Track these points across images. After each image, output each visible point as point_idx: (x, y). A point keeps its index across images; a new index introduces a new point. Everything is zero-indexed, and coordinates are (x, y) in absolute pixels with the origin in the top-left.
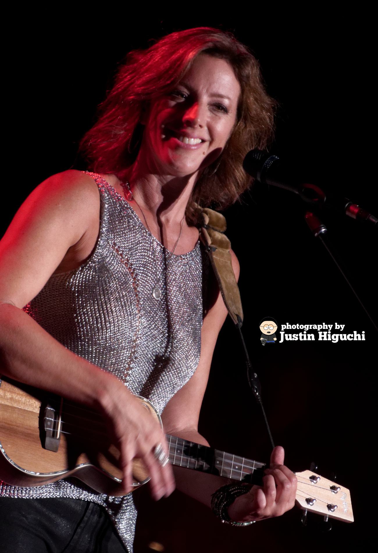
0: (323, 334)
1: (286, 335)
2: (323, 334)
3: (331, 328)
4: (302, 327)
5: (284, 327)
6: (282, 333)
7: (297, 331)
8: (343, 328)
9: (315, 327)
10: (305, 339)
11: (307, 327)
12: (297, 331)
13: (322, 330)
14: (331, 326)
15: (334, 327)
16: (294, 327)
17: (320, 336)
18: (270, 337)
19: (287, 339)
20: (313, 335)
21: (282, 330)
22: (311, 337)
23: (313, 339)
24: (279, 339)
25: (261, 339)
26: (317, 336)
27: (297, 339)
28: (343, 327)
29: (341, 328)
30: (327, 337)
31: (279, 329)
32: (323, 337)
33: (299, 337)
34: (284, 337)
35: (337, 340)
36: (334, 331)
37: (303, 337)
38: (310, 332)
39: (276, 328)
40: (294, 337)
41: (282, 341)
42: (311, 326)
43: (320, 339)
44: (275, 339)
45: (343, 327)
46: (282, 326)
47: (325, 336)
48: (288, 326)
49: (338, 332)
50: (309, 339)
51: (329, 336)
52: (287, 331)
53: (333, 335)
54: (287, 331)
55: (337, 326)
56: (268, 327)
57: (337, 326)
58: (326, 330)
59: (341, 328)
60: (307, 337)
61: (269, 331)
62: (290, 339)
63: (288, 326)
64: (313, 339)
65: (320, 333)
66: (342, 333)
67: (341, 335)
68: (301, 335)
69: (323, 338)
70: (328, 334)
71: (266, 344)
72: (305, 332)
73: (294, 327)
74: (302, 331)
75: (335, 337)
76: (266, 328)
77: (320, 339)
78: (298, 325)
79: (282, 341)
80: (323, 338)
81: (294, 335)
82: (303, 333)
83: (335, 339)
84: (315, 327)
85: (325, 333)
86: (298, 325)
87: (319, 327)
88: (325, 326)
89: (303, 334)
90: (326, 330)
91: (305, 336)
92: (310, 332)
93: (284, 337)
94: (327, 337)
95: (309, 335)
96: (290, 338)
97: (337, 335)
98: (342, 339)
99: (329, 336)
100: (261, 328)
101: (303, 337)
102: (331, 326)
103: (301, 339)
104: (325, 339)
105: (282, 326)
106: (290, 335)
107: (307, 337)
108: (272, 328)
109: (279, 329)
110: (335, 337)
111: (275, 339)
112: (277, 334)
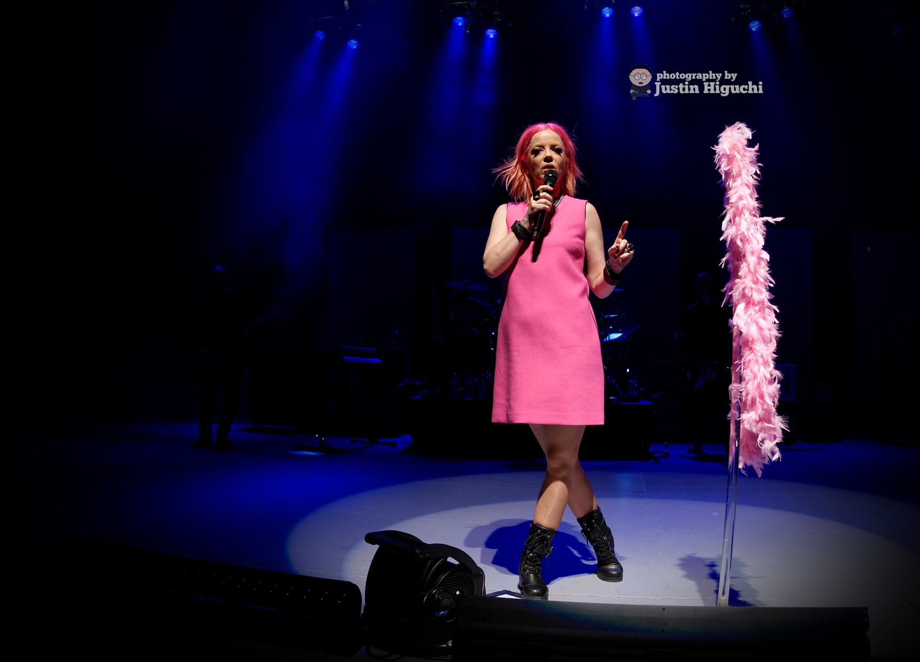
0: (709, 85)
1: (663, 87)
2: (709, 85)
3: (719, 78)
4: (683, 76)
5: (659, 76)
6: (658, 84)
8: (734, 78)
9: (699, 76)
10: (687, 91)
11: (689, 77)
12: (676, 82)
13: (708, 80)
14: (719, 76)
16: (673, 76)
17: (706, 88)
18: (642, 89)
19: (664, 92)
20: (696, 87)
22: (694, 89)
23: (697, 91)
24: (654, 91)
25: (631, 91)
26: (702, 88)
27: (676, 91)
28: (734, 76)
30: (715, 89)
31: (654, 79)
32: (709, 89)
34: (661, 89)
35: (727, 94)
36: (723, 82)
37: (684, 89)
38: (692, 82)
40: (674, 90)
41: (657, 94)
43: (706, 91)
44: (649, 92)
45: (734, 76)
47: (712, 88)
48: (665, 75)
49: (729, 82)
50: (692, 92)
51: (717, 87)
52: (664, 82)
53: (723, 87)
54: (664, 82)
55: (727, 76)
56: (640, 77)
57: (727, 76)
60: (689, 89)
62: (668, 91)
64: (697, 91)
65: (706, 84)
66: (734, 83)
67: (732, 87)
68: (681, 86)
69: (709, 90)
70: (717, 84)
71: (638, 98)
73: (673, 76)
74: (683, 81)
76: (637, 78)
77: (706, 91)
78: (677, 74)
79: (657, 94)
80: (709, 90)
81: (672, 87)
83: (725, 91)
84: (699, 76)
85: (712, 84)
86: (677, 74)
87: (705, 76)
88: (712, 75)
89: (683, 84)
91: (687, 87)
92: (692, 82)
93: (661, 89)
94: (715, 89)
95: (692, 87)
96: (668, 90)
97: (727, 87)
98: (733, 92)
99: (717, 87)
100: (631, 78)
101: (684, 89)
102: (719, 76)
103: (682, 92)
104: (712, 91)
106: (668, 87)
107: (689, 89)
108: (644, 78)
109: (654, 79)
111: (649, 92)
112: (652, 85)
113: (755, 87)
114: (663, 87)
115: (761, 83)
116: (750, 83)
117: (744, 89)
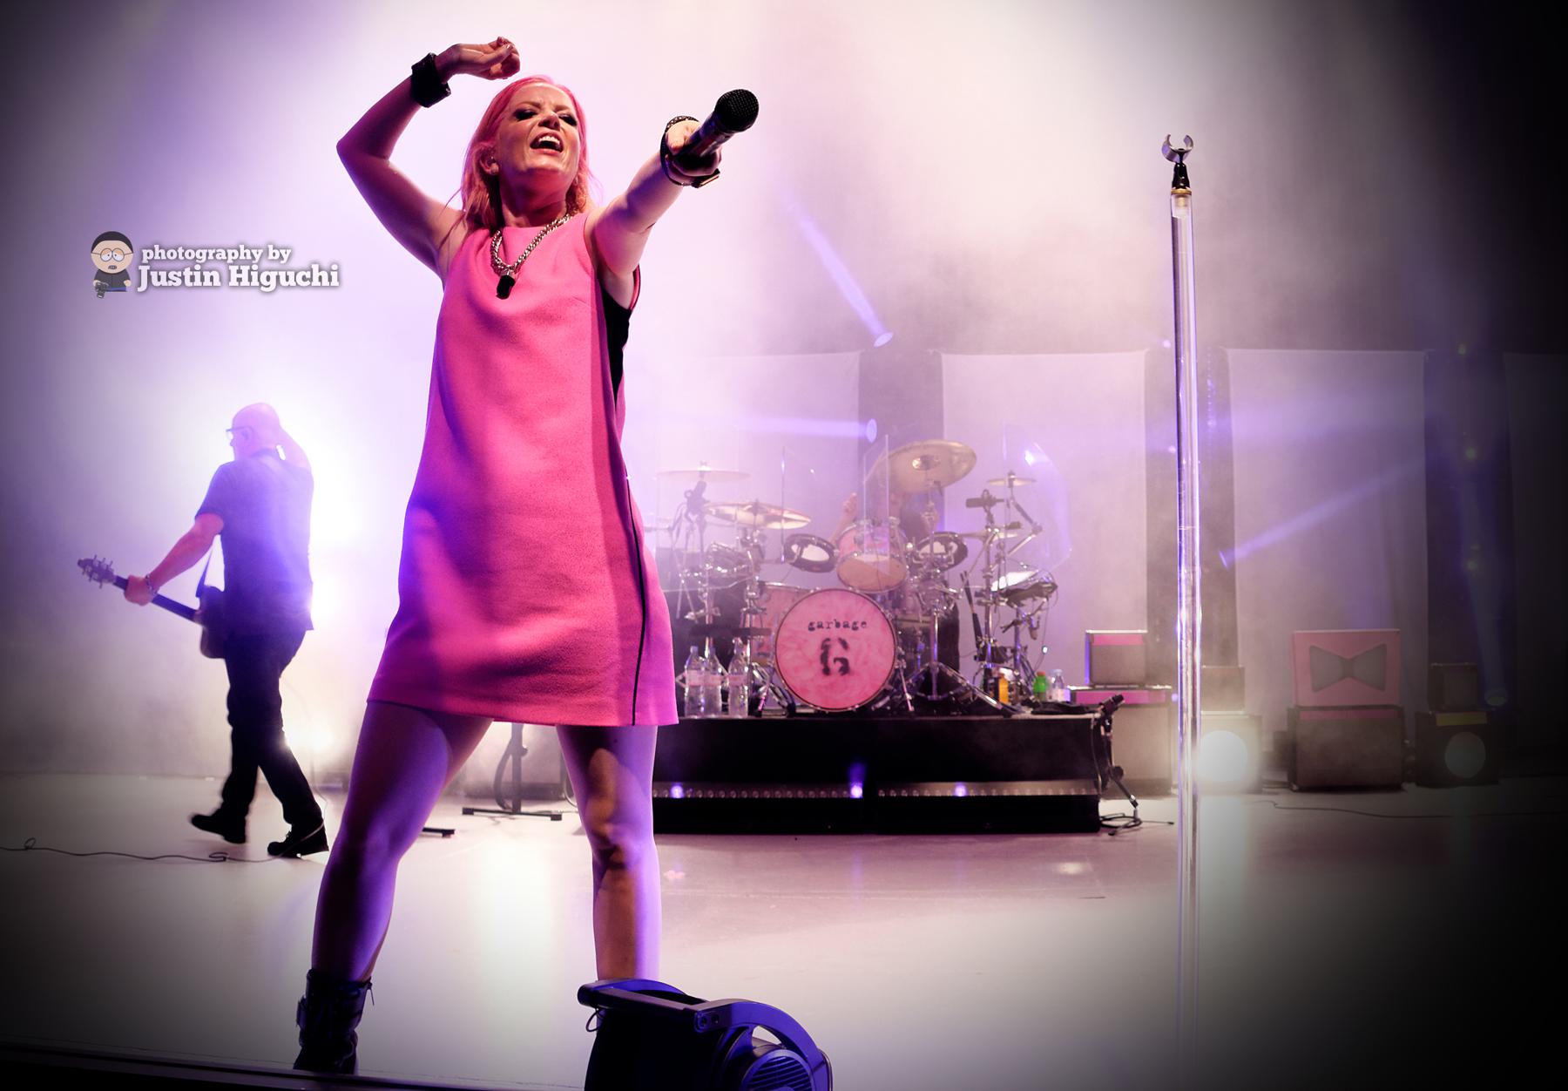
0: (239, 271)
2: (239, 271)
6: (144, 269)
13: (235, 262)
15: (267, 251)
16: (172, 254)
17: (234, 276)
19: (155, 282)
20: (216, 275)
23: (217, 282)
29: (281, 257)
30: (250, 279)
33: (183, 278)
34: (149, 277)
37: (192, 279)
43: (234, 282)
46: (145, 252)
47: (244, 276)
58: (249, 263)
59: (281, 257)
60: (202, 279)
61: (112, 263)
62: (163, 282)
69: (239, 280)
75: (268, 278)
76: (105, 257)
78: (181, 250)
80: (239, 280)
81: (171, 275)
82: (193, 270)
86: (181, 250)
90: (246, 262)
91: (197, 275)
93: (149, 277)
94: (250, 279)
101: (192, 279)
103: (188, 282)
105: (145, 252)
107: (202, 279)
108: (119, 257)
110: (268, 278)
113: (325, 275)
114: (154, 275)
115: (335, 267)
117: (304, 279)
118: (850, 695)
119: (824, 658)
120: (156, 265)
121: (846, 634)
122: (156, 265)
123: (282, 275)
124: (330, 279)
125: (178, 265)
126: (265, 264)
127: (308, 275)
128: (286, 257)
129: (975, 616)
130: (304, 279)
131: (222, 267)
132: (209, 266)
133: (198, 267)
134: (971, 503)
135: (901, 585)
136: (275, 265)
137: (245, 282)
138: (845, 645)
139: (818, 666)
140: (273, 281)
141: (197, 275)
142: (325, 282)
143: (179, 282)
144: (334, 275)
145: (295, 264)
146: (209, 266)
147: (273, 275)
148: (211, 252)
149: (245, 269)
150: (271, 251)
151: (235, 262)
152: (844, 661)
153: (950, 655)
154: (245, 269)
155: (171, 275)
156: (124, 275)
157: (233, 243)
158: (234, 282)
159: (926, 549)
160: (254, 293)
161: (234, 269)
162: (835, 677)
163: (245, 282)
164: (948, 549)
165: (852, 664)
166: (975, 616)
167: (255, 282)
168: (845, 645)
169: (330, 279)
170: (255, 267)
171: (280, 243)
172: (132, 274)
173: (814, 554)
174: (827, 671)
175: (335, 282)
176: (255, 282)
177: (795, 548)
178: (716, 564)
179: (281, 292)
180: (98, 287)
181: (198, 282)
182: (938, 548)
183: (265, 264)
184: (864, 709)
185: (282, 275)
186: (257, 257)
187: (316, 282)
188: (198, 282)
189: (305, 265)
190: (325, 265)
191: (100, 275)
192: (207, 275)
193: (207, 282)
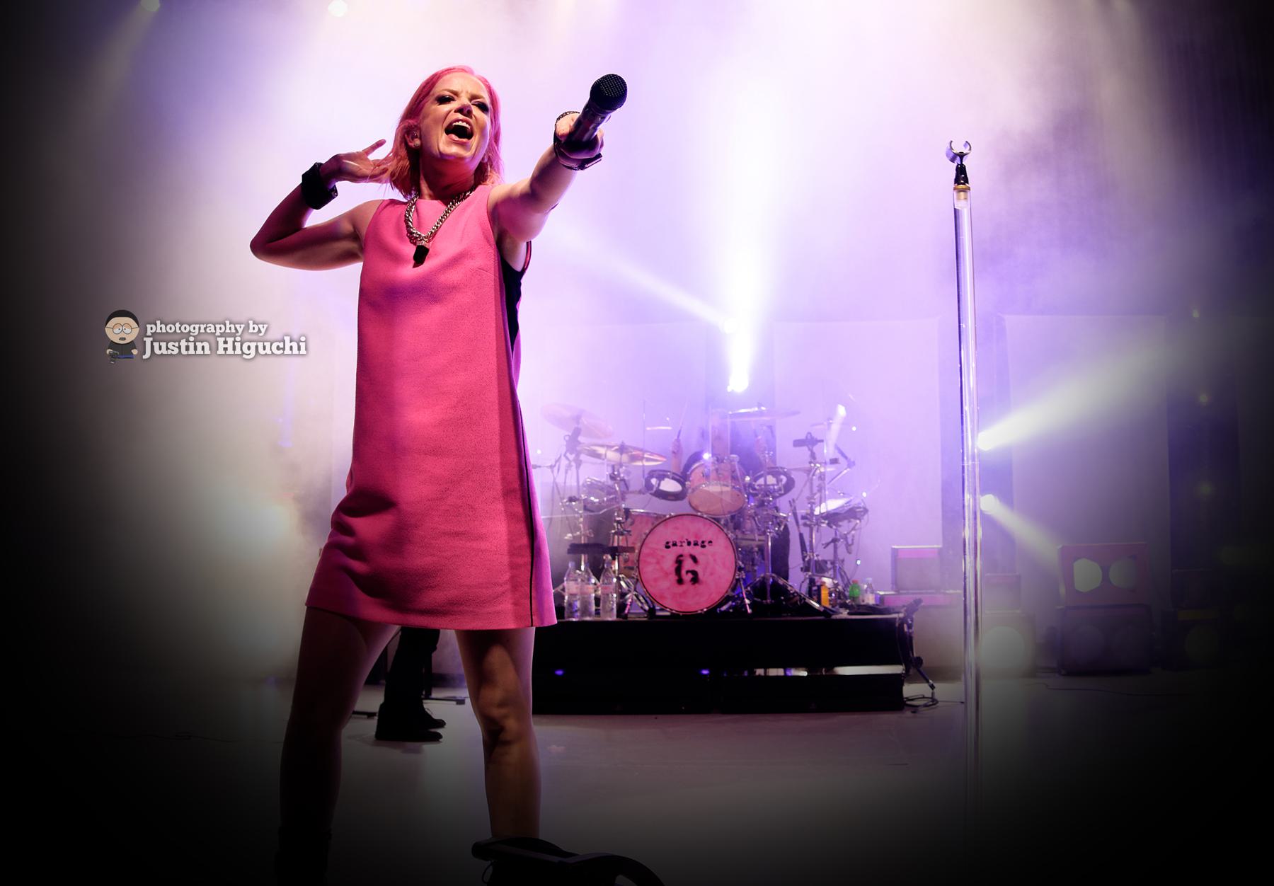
0: (225, 342)
2: (225, 342)
3: (240, 331)
6: (148, 341)
7: (176, 337)
8: (263, 330)
12: (176, 337)
13: (222, 335)
15: (248, 325)
16: (170, 329)
17: (221, 346)
19: (157, 351)
20: (206, 345)
21: (149, 333)
23: (207, 351)
26: (214, 348)
29: (259, 331)
30: (234, 349)
31: (143, 333)
33: (179, 347)
34: (152, 347)
37: (187, 348)
39: (136, 331)
42: (203, 327)
43: (221, 351)
47: (230, 346)
48: (160, 327)
50: (199, 351)
51: (238, 345)
58: (234, 335)
59: (259, 331)
60: (195, 348)
61: (122, 335)
62: (164, 351)
63: (160, 327)
65: (221, 340)
69: (225, 349)
72: (192, 339)
75: (249, 348)
76: (117, 331)
78: (178, 325)
80: (225, 349)
81: (170, 345)
82: (188, 341)
84: (211, 329)
86: (178, 325)
90: (234, 335)
91: (191, 345)
93: (152, 347)
94: (234, 349)
96: (162, 349)
97: (253, 345)
98: (261, 350)
99: (238, 345)
100: (108, 331)
101: (187, 348)
103: (184, 351)
107: (195, 348)
108: (128, 331)
110: (249, 348)
113: (295, 345)
114: (156, 345)
115: (303, 339)
116: (287, 339)
117: (278, 348)
118: (698, 601)
119: (678, 570)
120: (158, 337)
121: (697, 551)
122: (158, 337)
123: (261, 345)
124: (299, 349)
125: (176, 337)
126: (246, 336)
127: (281, 345)
128: (263, 330)
129: (801, 535)
130: (278, 348)
131: (211, 338)
132: (201, 337)
133: (192, 339)
134: (798, 443)
135: (741, 511)
136: (254, 337)
137: (230, 351)
138: (694, 559)
139: (674, 577)
140: (253, 349)
141: (191, 345)
142: (295, 351)
143: (176, 351)
144: (303, 345)
145: (270, 336)
146: (201, 337)
147: (253, 345)
148: (203, 327)
149: (230, 340)
150: (251, 326)
151: (222, 335)
152: (695, 573)
153: (781, 568)
154: (230, 340)
155: (170, 345)
156: (132, 345)
157: (220, 319)
158: (221, 351)
159: (761, 481)
160: (238, 359)
161: (221, 340)
162: (687, 586)
163: (230, 351)
164: (779, 481)
165: (700, 575)
166: (801, 535)
167: (238, 351)
168: (694, 559)
169: (299, 349)
170: (238, 339)
171: (258, 320)
172: (138, 344)
173: (670, 486)
174: (680, 581)
175: (303, 351)
176: (238, 351)
177: (654, 481)
178: (590, 494)
179: (259, 359)
180: (110, 355)
181: (192, 351)
182: (771, 480)
183: (246, 336)
184: (712, 611)
185: (261, 345)
186: (240, 331)
187: (287, 351)
188: (192, 351)
189: (279, 337)
190: (295, 337)
191: (113, 345)
192: (199, 345)
193: (199, 351)
